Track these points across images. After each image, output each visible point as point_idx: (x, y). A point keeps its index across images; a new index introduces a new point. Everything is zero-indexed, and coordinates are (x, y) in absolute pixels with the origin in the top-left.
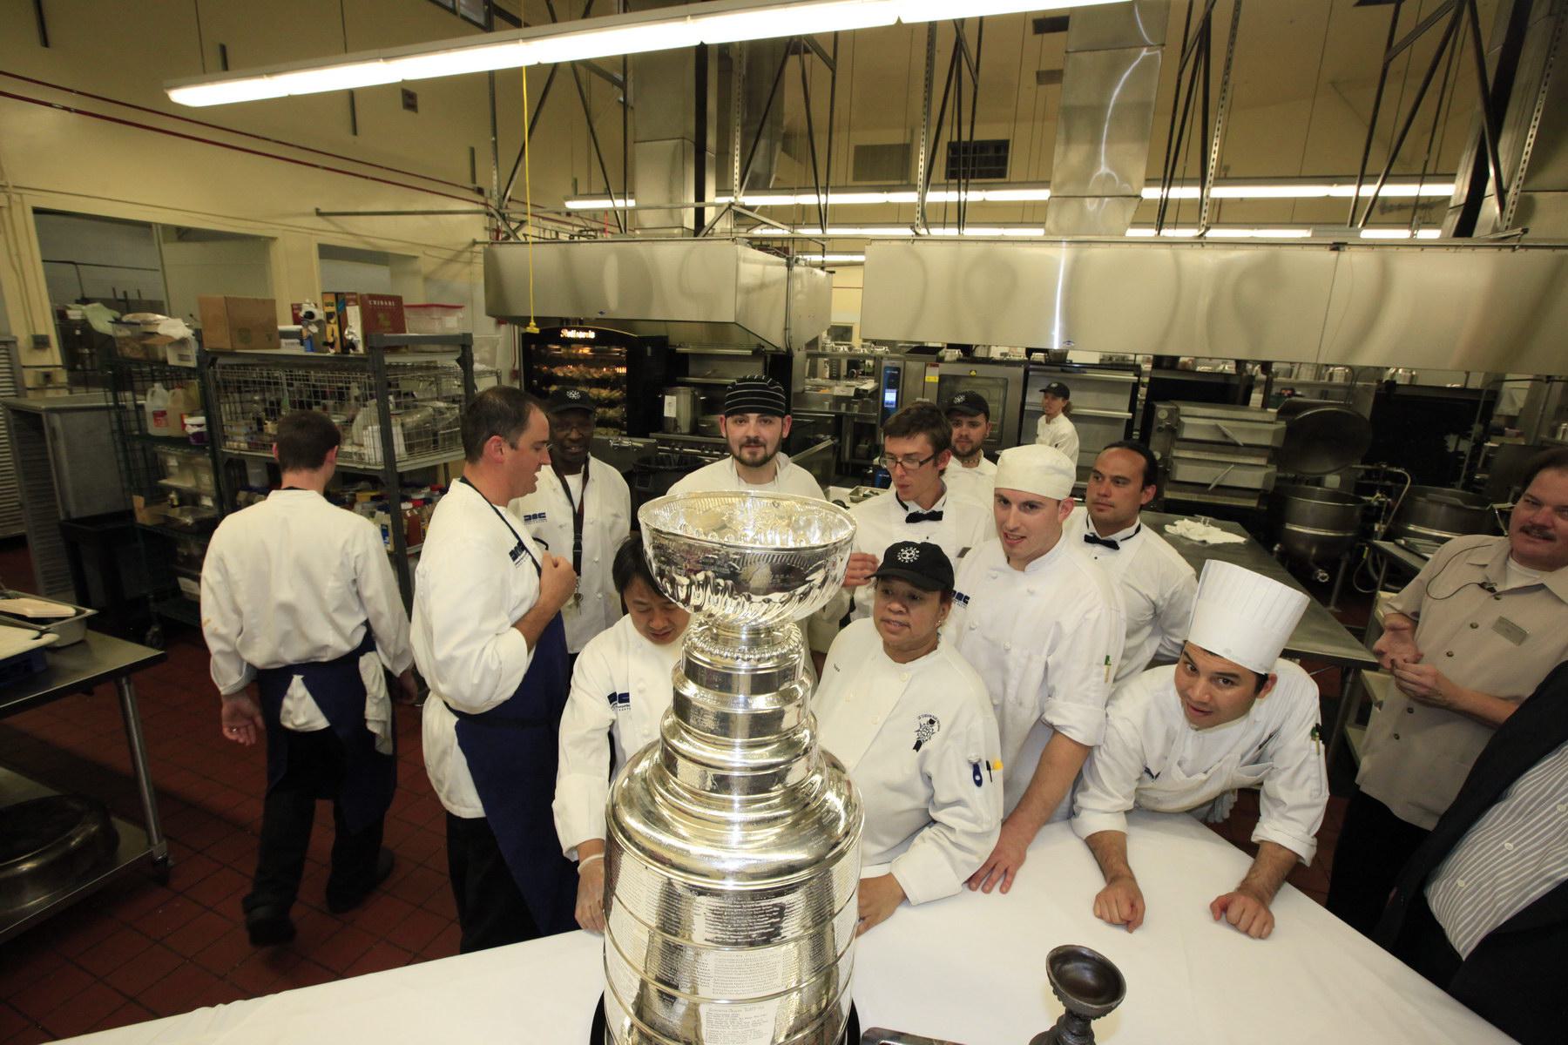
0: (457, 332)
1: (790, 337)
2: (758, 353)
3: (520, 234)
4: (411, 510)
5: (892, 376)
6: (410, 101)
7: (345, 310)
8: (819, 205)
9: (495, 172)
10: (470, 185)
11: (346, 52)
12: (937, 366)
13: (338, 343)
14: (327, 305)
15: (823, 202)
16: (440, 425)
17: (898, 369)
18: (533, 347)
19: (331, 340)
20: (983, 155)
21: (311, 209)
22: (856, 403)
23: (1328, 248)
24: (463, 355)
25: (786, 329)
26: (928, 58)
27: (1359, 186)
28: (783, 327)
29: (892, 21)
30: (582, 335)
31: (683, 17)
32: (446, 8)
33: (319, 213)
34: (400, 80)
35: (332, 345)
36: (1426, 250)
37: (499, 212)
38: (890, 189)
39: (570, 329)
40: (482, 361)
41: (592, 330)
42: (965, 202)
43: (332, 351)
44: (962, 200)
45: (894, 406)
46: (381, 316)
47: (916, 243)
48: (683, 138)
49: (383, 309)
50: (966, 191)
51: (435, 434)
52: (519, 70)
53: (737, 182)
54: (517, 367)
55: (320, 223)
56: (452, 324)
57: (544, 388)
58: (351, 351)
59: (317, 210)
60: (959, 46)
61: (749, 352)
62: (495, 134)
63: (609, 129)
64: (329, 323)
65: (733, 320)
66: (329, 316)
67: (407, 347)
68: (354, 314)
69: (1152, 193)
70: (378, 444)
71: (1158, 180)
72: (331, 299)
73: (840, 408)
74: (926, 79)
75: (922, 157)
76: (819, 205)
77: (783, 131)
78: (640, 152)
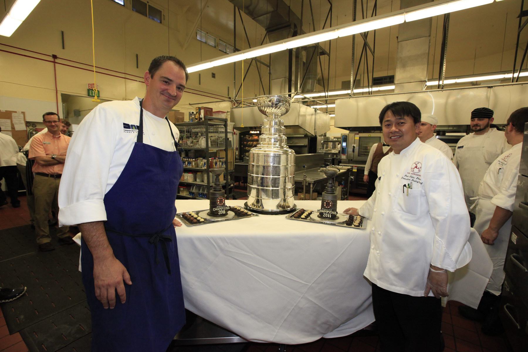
0: (225, 118)
1: (316, 132)
2: (306, 136)
3: (240, 105)
4: (211, 159)
5: (344, 138)
6: (214, 76)
7: (200, 111)
8: (326, 95)
9: (234, 90)
10: (227, 97)
11: (201, 61)
12: (358, 134)
13: (198, 119)
14: (197, 110)
15: (327, 95)
16: (219, 141)
17: (346, 136)
18: (242, 136)
19: (197, 118)
20: (386, 81)
21: (188, 103)
22: (338, 155)
23: (487, 88)
24: (225, 123)
25: (315, 129)
26: (353, 48)
27: (513, 74)
28: (314, 129)
29: (337, 37)
30: (256, 132)
31: (282, 43)
32: (224, 52)
33: (190, 104)
34: (213, 66)
35: (197, 119)
36: (523, 85)
37: (235, 100)
38: (348, 90)
39: (252, 131)
40: (229, 129)
41: (259, 131)
42: (372, 91)
43: (197, 121)
44: (370, 90)
45: (345, 147)
46: (208, 112)
47: (350, 98)
48: (285, 78)
49: (209, 111)
50: (372, 88)
51: (218, 143)
52: (242, 60)
53: (299, 87)
54: (237, 147)
55: (190, 107)
56: (223, 116)
57: (245, 148)
58: (201, 120)
59: (189, 103)
60: (365, 45)
61: (303, 136)
62: (235, 80)
63: (266, 80)
64: (197, 114)
65: (297, 125)
66: (197, 112)
67: (213, 120)
68: (202, 112)
69: (436, 83)
70: (205, 143)
71: (438, 78)
72: (198, 109)
73: (334, 157)
74: (352, 53)
75: (352, 74)
76: (326, 95)
77: (317, 79)
78: (272, 82)
